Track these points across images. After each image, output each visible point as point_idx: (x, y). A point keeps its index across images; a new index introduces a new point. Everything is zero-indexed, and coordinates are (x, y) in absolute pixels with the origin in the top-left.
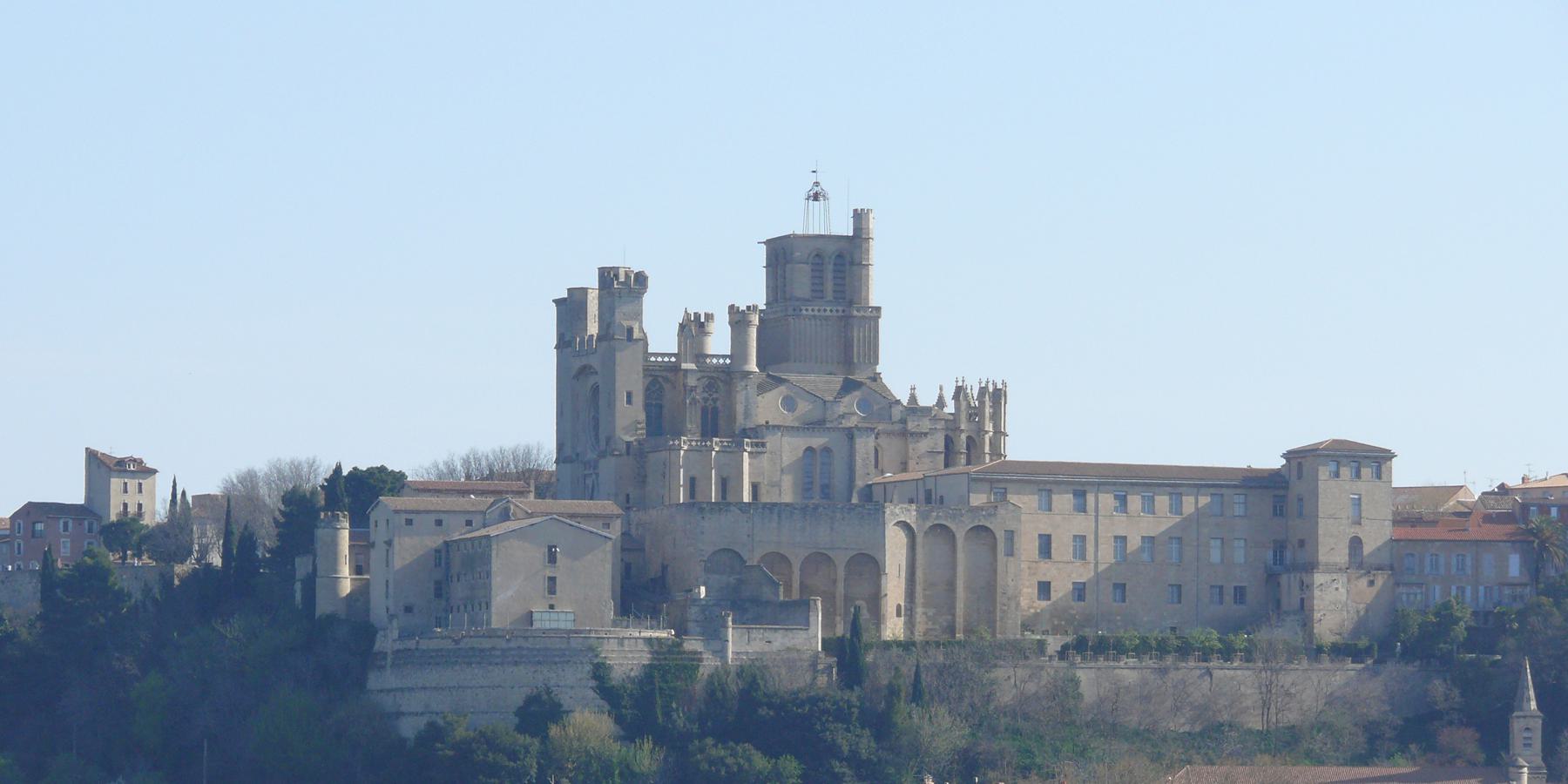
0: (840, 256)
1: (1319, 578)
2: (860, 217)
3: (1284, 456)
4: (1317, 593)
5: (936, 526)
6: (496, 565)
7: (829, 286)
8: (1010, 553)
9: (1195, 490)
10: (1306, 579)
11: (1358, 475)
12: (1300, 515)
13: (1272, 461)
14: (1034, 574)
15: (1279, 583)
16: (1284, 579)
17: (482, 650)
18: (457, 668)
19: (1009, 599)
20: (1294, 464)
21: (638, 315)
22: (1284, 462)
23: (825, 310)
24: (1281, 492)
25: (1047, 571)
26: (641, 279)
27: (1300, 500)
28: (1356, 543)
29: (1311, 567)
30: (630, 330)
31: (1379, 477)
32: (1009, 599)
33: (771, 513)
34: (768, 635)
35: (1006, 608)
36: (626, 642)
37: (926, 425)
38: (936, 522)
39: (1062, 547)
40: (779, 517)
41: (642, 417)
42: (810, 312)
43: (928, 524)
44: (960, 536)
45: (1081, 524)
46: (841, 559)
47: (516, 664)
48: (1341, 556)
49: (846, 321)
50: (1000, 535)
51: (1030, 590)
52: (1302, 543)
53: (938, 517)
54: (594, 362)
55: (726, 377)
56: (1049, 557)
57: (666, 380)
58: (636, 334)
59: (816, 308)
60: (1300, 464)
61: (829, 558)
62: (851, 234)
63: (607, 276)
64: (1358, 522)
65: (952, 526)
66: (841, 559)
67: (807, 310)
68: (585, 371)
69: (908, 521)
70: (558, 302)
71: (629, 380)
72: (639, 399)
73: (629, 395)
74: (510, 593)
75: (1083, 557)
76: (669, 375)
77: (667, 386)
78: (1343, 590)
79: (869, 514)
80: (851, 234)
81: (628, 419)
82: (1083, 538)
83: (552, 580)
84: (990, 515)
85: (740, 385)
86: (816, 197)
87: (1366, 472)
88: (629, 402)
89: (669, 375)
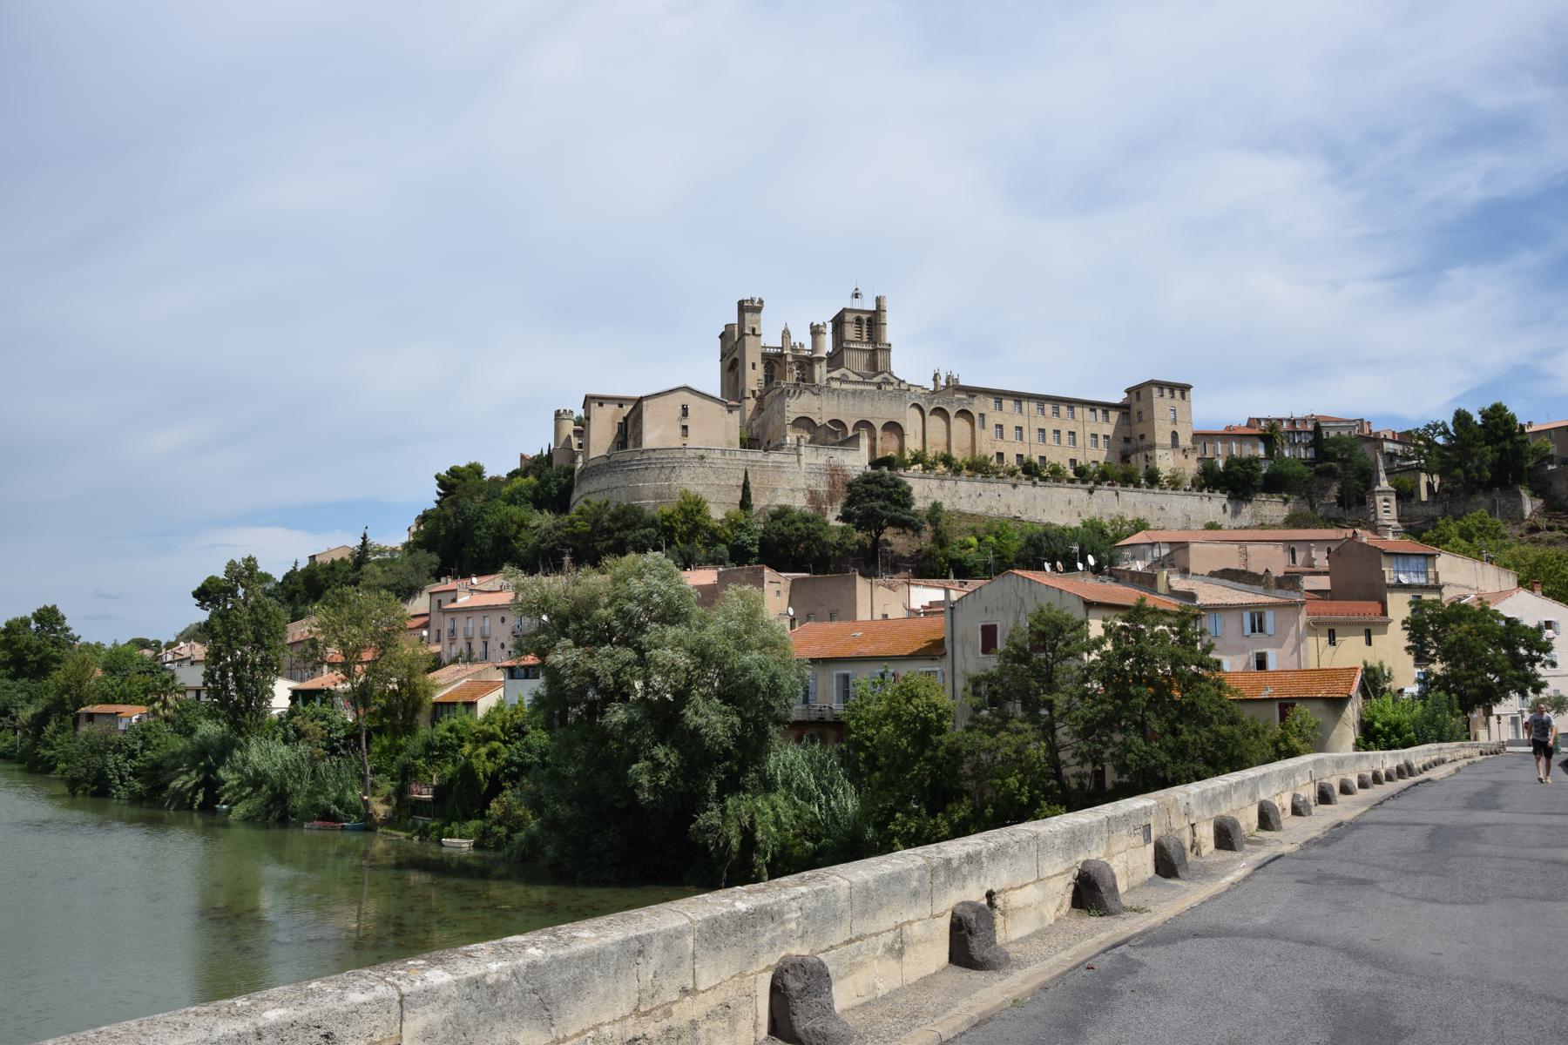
0: (869, 320)
1: (1158, 452)
2: (878, 300)
3: (1129, 391)
4: (1158, 461)
6: (646, 416)
7: (865, 334)
8: (983, 427)
10: (1149, 453)
11: (1173, 397)
12: (1140, 420)
13: (1118, 397)
15: (1129, 462)
16: (1133, 458)
17: (624, 462)
18: (608, 475)
20: (1134, 394)
21: (758, 322)
22: (1126, 395)
24: (1126, 411)
25: (1001, 446)
26: (761, 302)
27: (1139, 413)
28: (1175, 435)
29: (1152, 447)
30: (754, 330)
31: (1183, 397)
34: (831, 453)
36: (727, 453)
37: (920, 391)
39: (1009, 432)
41: (762, 377)
43: (932, 407)
44: (952, 414)
45: (1020, 420)
46: (878, 425)
47: (647, 468)
48: (1168, 441)
49: (874, 352)
52: (1142, 437)
54: (736, 355)
55: (806, 364)
56: (1002, 437)
57: (776, 361)
58: (757, 332)
60: (1138, 393)
61: (871, 424)
62: (875, 309)
63: (743, 308)
64: (1175, 421)
65: (948, 410)
68: (735, 360)
70: (720, 337)
71: (752, 356)
72: (760, 367)
73: (754, 365)
74: (655, 435)
75: (1021, 439)
76: (778, 359)
77: (776, 366)
78: (1171, 460)
80: (875, 309)
81: (754, 378)
82: (1020, 428)
83: (685, 428)
85: (817, 367)
86: (857, 297)
87: (1177, 393)
88: (754, 368)
89: (778, 359)
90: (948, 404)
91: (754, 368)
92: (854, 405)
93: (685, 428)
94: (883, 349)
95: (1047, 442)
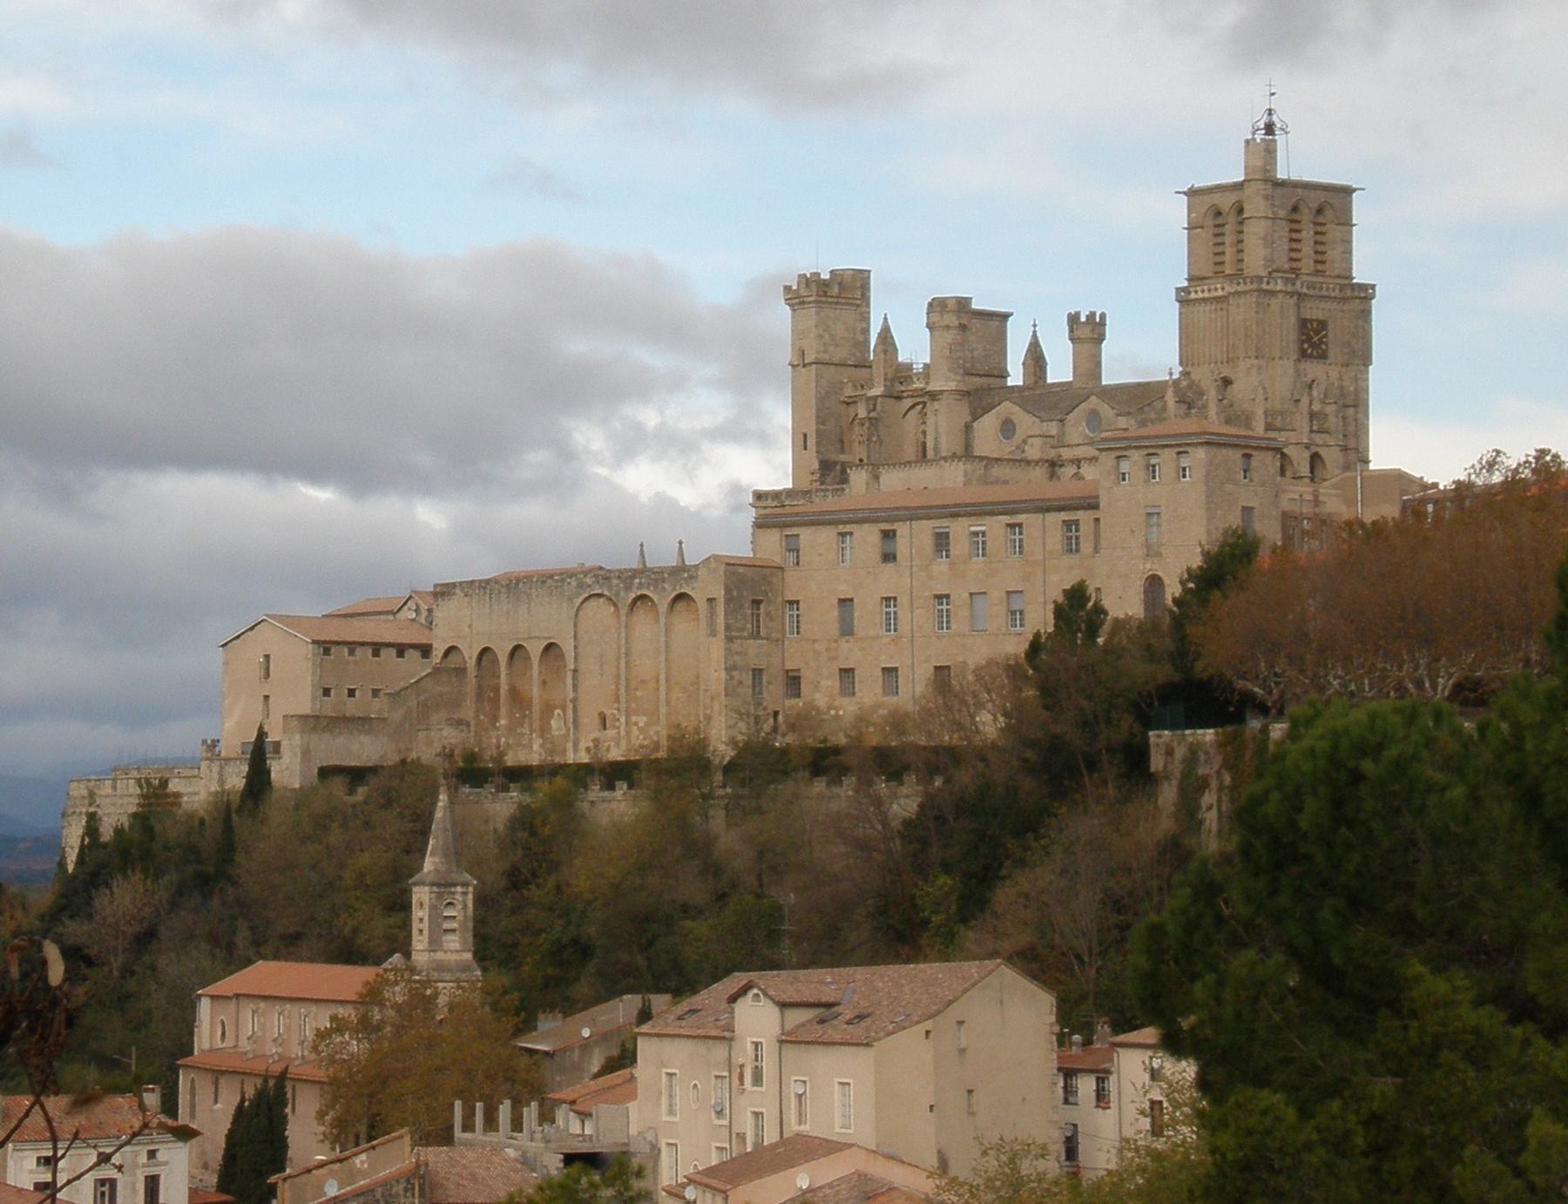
5: (635, 601)
9: (1041, 516)
14: (834, 658)
19: (712, 699)
23: (1216, 289)
25: (850, 654)
32: (712, 699)
33: (485, 593)
35: (708, 711)
38: (639, 593)
39: (867, 615)
40: (490, 598)
42: (1200, 295)
46: (535, 649)
50: (702, 605)
51: (829, 683)
53: (641, 586)
59: (1206, 288)
66: (535, 649)
67: (1196, 292)
69: (606, 593)
79: (557, 587)
84: (691, 577)
90: (656, 587)
91: (805, 449)
92: (508, 613)
93: (267, 697)
94: (1237, 293)
95: (954, 626)
